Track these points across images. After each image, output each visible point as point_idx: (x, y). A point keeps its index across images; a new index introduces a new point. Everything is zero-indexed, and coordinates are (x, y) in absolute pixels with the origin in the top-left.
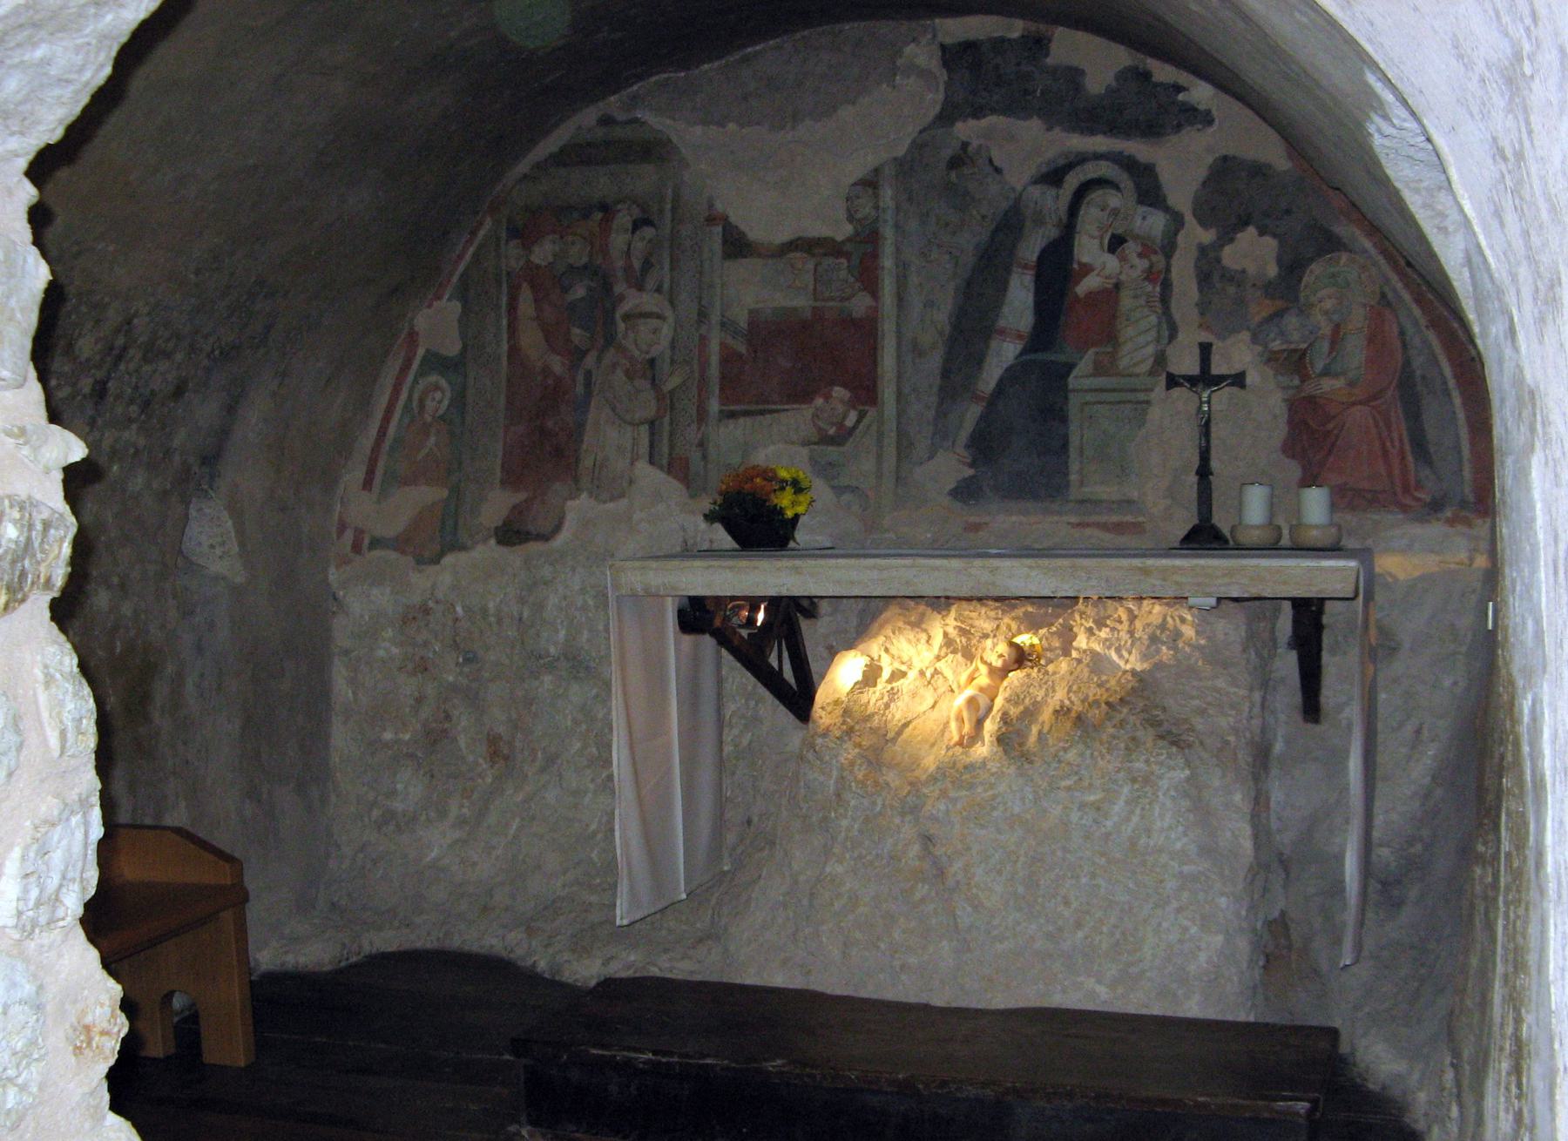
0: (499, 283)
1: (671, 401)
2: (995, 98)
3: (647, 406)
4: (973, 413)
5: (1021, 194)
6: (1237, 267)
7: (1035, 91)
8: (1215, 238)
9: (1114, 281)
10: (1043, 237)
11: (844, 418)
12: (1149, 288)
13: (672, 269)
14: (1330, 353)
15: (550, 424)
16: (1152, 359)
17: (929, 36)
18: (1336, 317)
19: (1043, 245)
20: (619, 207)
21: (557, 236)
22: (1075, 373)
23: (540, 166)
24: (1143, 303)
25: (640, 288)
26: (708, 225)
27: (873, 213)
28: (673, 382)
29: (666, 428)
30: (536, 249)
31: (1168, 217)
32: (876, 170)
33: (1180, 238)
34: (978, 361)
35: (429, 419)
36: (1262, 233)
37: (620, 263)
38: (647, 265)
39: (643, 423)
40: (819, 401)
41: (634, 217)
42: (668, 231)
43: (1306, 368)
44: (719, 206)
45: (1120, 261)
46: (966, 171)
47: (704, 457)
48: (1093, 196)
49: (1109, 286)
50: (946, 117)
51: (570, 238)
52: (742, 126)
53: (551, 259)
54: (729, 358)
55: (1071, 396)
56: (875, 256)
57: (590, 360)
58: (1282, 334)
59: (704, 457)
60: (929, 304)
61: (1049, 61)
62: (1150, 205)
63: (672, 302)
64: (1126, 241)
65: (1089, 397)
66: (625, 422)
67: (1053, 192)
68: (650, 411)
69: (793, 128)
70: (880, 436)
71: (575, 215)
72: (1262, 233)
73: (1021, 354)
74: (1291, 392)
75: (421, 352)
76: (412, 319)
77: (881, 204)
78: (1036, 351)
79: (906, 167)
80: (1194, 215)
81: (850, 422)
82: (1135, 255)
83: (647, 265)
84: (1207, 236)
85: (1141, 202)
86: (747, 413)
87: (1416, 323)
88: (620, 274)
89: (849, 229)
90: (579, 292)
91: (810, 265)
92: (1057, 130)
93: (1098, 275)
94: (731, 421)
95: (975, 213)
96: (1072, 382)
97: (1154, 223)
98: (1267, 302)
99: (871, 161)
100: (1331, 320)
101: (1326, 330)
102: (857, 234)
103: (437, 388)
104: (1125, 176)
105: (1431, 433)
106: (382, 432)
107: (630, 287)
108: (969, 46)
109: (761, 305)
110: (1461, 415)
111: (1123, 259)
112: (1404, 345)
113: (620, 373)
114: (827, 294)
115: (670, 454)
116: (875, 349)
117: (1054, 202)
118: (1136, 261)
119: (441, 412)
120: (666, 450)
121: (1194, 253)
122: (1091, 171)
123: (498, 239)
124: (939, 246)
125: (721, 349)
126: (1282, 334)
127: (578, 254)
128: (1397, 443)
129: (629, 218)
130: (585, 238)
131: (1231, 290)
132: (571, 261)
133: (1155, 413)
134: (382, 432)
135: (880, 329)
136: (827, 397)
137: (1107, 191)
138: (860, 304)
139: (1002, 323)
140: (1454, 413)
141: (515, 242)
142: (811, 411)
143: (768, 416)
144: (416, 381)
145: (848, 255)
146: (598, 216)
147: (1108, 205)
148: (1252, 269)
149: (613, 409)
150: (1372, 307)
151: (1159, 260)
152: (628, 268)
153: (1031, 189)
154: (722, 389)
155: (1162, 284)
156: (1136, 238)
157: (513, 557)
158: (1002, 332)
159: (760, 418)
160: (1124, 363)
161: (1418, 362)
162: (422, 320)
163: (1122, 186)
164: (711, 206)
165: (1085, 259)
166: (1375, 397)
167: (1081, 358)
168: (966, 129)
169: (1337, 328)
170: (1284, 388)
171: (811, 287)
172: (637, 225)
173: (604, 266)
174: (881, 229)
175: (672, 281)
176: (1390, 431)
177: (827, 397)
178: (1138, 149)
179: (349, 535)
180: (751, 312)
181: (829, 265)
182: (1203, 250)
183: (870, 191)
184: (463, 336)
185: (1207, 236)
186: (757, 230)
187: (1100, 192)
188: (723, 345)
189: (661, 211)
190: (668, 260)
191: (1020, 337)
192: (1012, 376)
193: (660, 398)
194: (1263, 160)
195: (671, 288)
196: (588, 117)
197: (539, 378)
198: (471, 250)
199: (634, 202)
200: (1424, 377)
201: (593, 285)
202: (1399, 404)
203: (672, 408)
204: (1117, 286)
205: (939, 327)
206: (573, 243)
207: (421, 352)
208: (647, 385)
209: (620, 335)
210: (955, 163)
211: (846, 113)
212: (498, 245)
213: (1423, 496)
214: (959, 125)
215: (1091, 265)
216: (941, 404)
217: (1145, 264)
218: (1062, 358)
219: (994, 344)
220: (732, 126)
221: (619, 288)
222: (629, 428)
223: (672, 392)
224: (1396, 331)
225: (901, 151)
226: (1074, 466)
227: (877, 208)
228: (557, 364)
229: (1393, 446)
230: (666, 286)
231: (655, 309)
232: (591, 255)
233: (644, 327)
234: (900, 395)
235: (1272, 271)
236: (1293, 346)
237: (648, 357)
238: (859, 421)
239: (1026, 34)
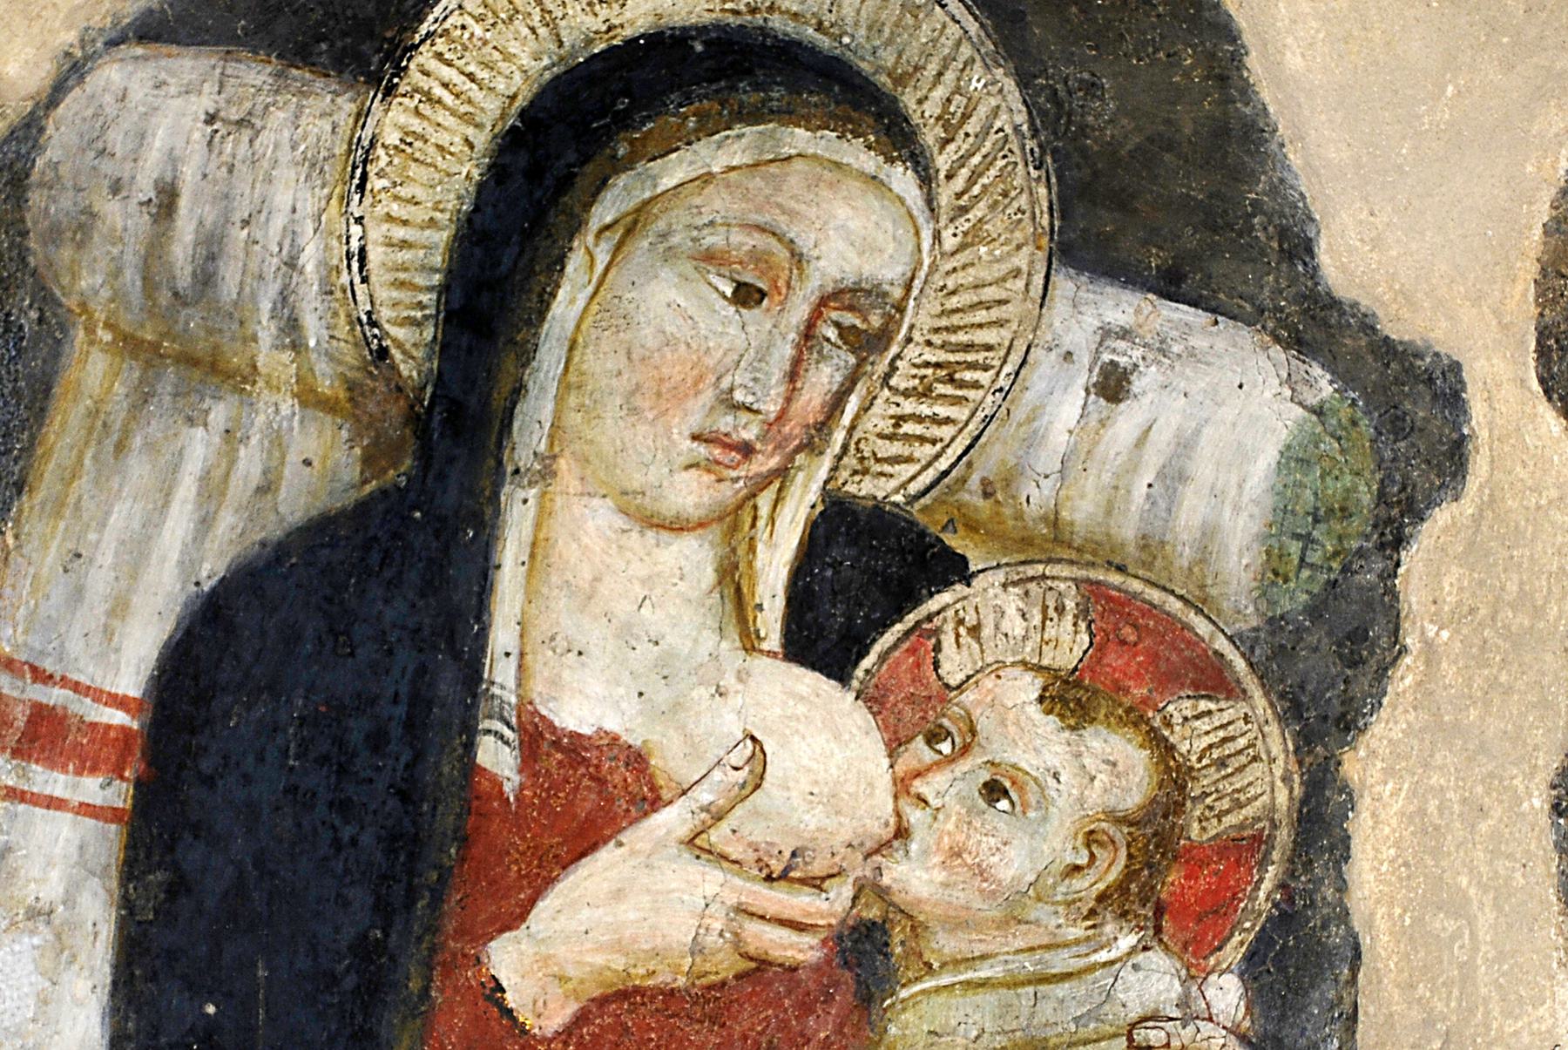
9: (831, 906)
10: (212, 490)
19: (212, 568)
31: (1324, 386)
45: (895, 745)
48: (674, 171)
49: (802, 949)
62: (1170, 286)
64: (955, 570)
82: (1027, 688)
93: (694, 844)
137: (799, 138)
155: (1253, 967)
215: (637, 760)
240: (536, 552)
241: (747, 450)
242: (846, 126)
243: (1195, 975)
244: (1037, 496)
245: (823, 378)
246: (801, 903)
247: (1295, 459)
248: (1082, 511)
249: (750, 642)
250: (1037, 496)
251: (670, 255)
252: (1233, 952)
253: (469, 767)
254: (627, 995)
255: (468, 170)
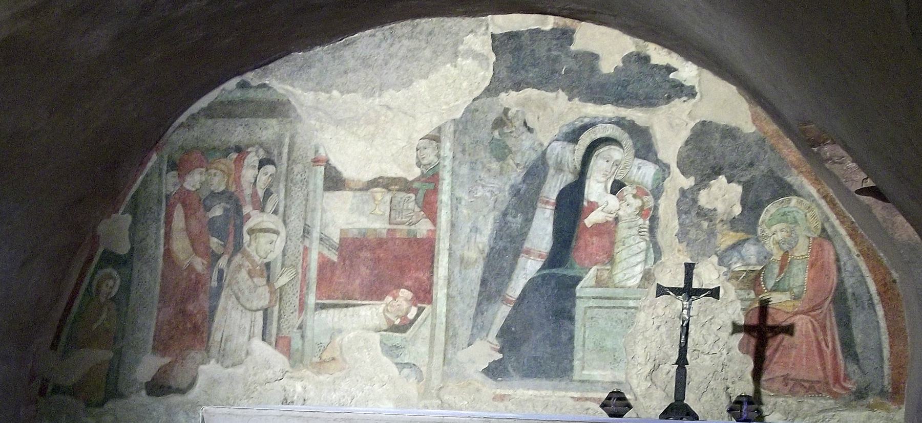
0: (159, 201)
1: (281, 295)
2: (531, 75)
3: (262, 298)
4: (502, 312)
5: (546, 149)
6: (708, 207)
7: (561, 71)
8: (693, 184)
11: (407, 313)
12: (641, 221)
13: (286, 198)
14: (780, 274)
15: (190, 307)
16: (641, 276)
17: (484, 29)
18: (785, 247)
20: (249, 150)
21: (203, 170)
22: (581, 284)
23: (193, 116)
24: (637, 233)
25: (263, 210)
26: (313, 166)
27: (436, 160)
28: (283, 281)
29: (276, 314)
30: (188, 179)
31: (658, 167)
32: (439, 129)
33: (667, 184)
34: (508, 274)
35: (103, 300)
36: (729, 182)
37: (248, 191)
38: (268, 193)
39: (259, 310)
40: (389, 299)
41: (261, 158)
42: (284, 167)
43: (760, 284)
44: (321, 151)
46: (506, 130)
47: (303, 337)
48: (601, 150)
49: (611, 219)
50: (492, 90)
51: (213, 171)
52: (342, 93)
53: (198, 186)
54: (325, 266)
55: (578, 301)
56: (435, 191)
57: (222, 263)
58: (742, 258)
59: (303, 337)
60: (475, 230)
61: (572, 48)
63: (284, 222)
64: (625, 185)
65: (592, 303)
66: (246, 308)
67: (571, 147)
68: (264, 303)
69: (380, 96)
70: (433, 327)
71: (218, 154)
72: (729, 182)
73: (539, 270)
74: (748, 303)
75: (101, 250)
76: (95, 227)
77: (442, 154)
78: (554, 267)
79: (463, 125)
80: (679, 167)
81: (411, 316)
83: (268, 193)
84: (688, 182)
85: (637, 156)
86: (335, 306)
87: (849, 252)
88: (248, 199)
89: (417, 172)
90: (217, 212)
91: (388, 198)
92: (576, 100)
94: (324, 311)
95: (511, 162)
96: (580, 290)
97: (646, 172)
98: (731, 233)
99: (436, 121)
100: (781, 248)
101: (777, 256)
102: (423, 175)
103: (110, 277)
104: (626, 135)
105: (858, 337)
106: (68, 309)
107: (254, 209)
108: (512, 36)
109: (350, 227)
110: (883, 324)
111: (621, 199)
112: (839, 269)
113: (244, 274)
114: (399, 220)
115: (277, 334)
116: (433, 262)
117: (573, 155)
118: (630, 198)
119: (113, 294)
120: (274, 331)
121: (676, 196)
122: (600, 132)
123: (161, 170)
124: (483, 186)
125: (319, 258)
126: (742, 258)
127: (218, 184)
128: (830, 345)
129: (256, 158)
130: (223, 171)
131: (705, 224)
132: (212, 188)
133: (642, 316)
134: (68, 309)
135: (436, 247)
136: (395, 298)
137: (612, 147)
138: (423, 228)
139: (527, 245)
140: (878, 322)
141: (175, 173)
142: (384, 306)
143: (351, 309)
144: (95, 272)
145: (416, 191)
146: (234, 156)
147: (612, 158)
148: (721, 207)
149: (238, 299)
150: (814, 239)
151: (650, 201)
152: (254, 194)
153: (555, 144)
154: (318, 288)
156: (632, 183)
157: (159, 405)
158: (528, 252)
159: (345, 309)
160: (619, 276)
161: (849, 282)
162: (102, 228)
163: (623, 143)
164: (317, 151)
165: (593, 199)
166: (813, 309)
167: (587, 273)
168: (509, 99)
169: (786, 253)
170: (742, 300)
171: (387, 213)
172: (262, 164)
173: (236, 193)
174: (441, 173)
175: (285, 207)
176: (825, 334)
177: (395, 298)
178: (637, 115)
179: (37, 384)
180: (341, 230)
181: (401, 198)
182: (683, 192)
183: (434, 143)
184: (132, 241)
185: (688, 182)
186: (348, 172)
187: (606, 148)
188: (321, 255)
189: (280, 154)
190: (284, 191)
191: (540, 256)
192: (533, 286)
193: (272, 293)
194: (733, 125)
195: (285, 211)
196: (232, 83)
197: (185, 273)
198: (141, 178)
199: (261, 147)
200: (854, 294)
201: (228, 206)
202: (833, 314)
203: (281, 299)
204: (617, 219)
205: (481, 246)
206: (215, 175)
207: (101, 250)
208: (263, 281)
209: (246, 245)
210: (500, 123)
211: (421, 86)
212: (160, 175)
213: (848, 385)
214: (503, 95)
215: (597, 203)
216: (479, 304)
217: (637, 203)
218: (570, 273)
219: (522, 260)
220: (335, 93)
221: (247, 209)
222: (249, 314)
223: (281, 288)
224: (832, 257)
225: (458, 116)
226: (578, 354)
227: (438, 156)
228: (199, 264)
229: (827, 347)
230: (281, 209)
231: (272, 226)
232: (228, 182)
233: (263, 239)
234: (449, 297)
235: (737, 210)
236: (751, 268)
237: (266, 261)
238: (418, 315)
239: (556, 27)
240: (589, 186)
241: (607, 175)
242: (617, 145)
243: (645, 221)
244: (632, 178)
245: (614, 168)
246: (610, 215)
247: (655, 174)
248: (636, 180)
249: (607, 193)
250: (632, 178)
251: (601, 158)
252: (648, 218)
253: (583, 204)
254: (597, 224)
255: (584, 151)
